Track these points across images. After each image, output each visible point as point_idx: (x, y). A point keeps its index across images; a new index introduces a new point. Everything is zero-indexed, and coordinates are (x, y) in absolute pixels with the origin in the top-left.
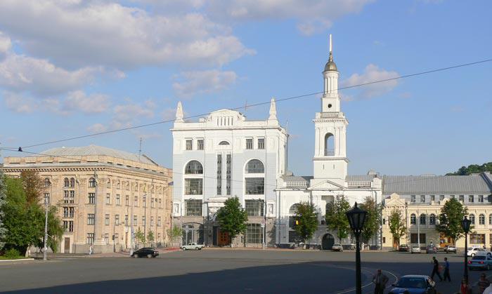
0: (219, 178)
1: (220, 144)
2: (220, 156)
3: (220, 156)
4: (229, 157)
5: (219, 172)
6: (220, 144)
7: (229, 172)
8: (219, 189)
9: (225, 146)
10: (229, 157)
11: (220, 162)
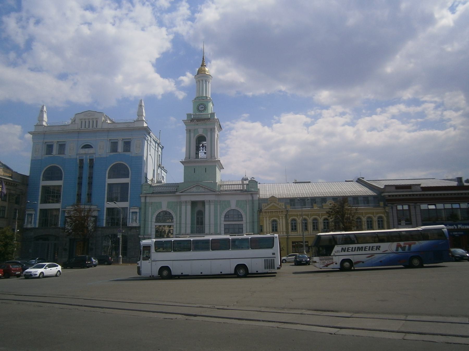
0: (80, 184)
1: (82, 148)
2: (81, 161)
3: (81, 161)
4: (91, 160)
5: (80, 178)
6: (82, 148)
7: (91, 178)
8: (79, 195)
9: (87, 150)
10: (91, 160)
11: (81, 167)
